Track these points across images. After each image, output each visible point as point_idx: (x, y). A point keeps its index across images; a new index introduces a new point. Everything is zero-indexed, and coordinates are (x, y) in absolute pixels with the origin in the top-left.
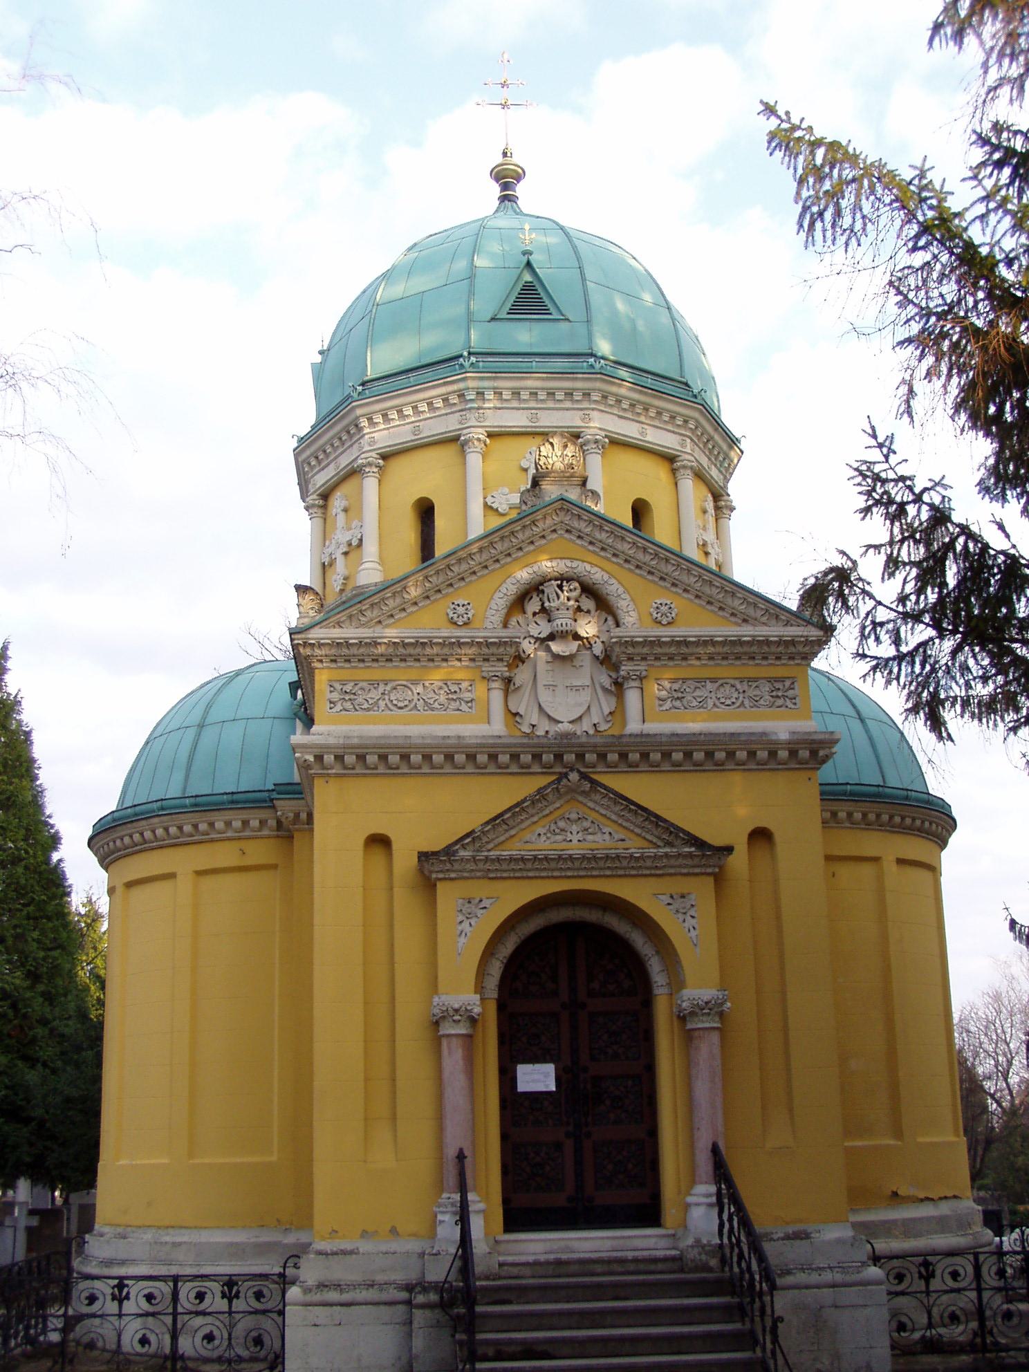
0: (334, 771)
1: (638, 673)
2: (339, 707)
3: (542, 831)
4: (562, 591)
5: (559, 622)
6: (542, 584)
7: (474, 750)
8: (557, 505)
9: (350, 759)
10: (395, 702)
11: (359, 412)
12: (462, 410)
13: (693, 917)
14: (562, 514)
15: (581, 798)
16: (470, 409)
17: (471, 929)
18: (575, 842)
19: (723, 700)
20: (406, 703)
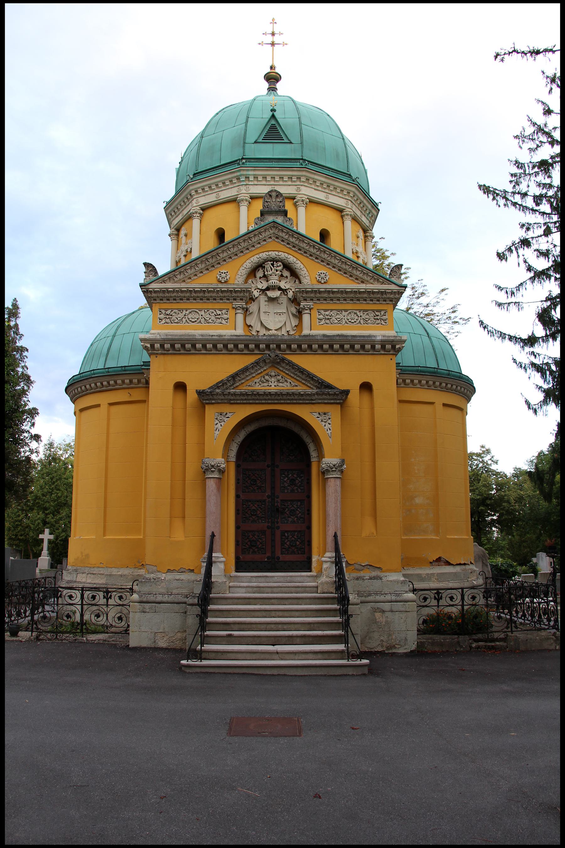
0: (160, 352)
1: (309, 306)
2: (164, 321)
3: (257, 381)
4: (274, 267)
5: (271, 281)
6: (264, 263)
7: (227, 342)
8: (272, 225)
9: (167, 346)
10: (190, 319)
11: (191, 188)
12: (239, 186)
13: (329, 424)
14: (274, 229)
15: (276, 366)
16: (242, 185)
17: (221, 427)
18: (273, 386)
19: (350, 320)
20: (196, 319)
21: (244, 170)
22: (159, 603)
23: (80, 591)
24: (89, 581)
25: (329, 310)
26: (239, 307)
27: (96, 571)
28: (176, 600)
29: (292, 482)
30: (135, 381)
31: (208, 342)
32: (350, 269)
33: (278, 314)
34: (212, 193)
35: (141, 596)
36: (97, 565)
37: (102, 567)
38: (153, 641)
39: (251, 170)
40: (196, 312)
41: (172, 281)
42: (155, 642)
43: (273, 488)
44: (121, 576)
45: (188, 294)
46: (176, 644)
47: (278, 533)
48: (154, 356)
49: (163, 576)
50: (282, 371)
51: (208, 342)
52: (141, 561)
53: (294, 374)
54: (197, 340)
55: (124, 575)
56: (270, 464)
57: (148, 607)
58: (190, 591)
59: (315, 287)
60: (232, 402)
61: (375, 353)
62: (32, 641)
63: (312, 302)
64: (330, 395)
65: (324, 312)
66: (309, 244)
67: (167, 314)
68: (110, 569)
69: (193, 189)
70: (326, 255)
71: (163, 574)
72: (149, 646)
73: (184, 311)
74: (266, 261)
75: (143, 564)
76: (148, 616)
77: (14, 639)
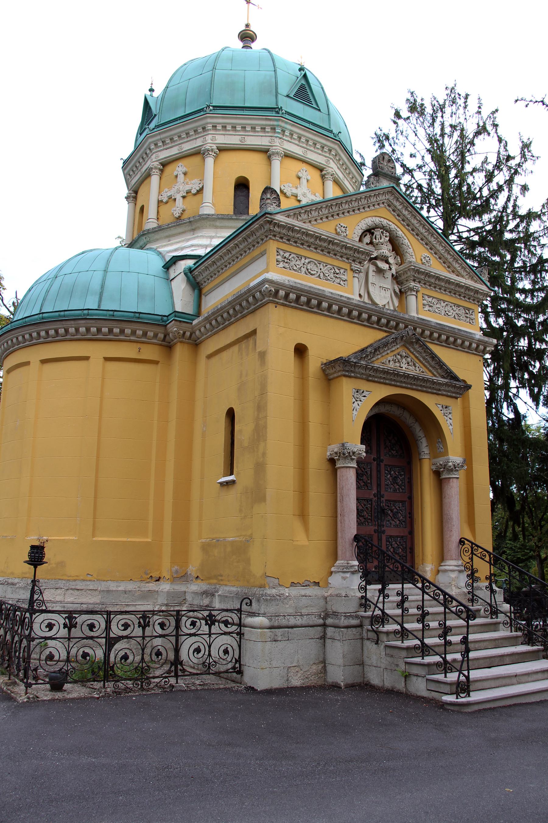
0: (281, 301)
1: (417, 288)
2: (281, 265)
3: (391, 359)
4: (383, 235)
5: (382, 251)
6: (374, 229)
7: (353, 307)
8: (390, 189)
9: (292, 296)
10: (310, 270)
11: (209, 120)
12: (272, 137)
13: (450, 419)
14: (390, 195)
15: (408, 346)
16: (276, 137)
17: (358, 407)
18: (404, 369)
19: (447, 312)
20: (315, 272)
21: (283, 121)
22: (292, 627)
23: (175, 617)
24: (69, 600)
25: (431, 297)
26: (357, 270)
27: (80, 585)
28: (311, 623)
29: (395, 479)
30: (150, 334)
31: (336, 302)
32: (451, 260)
33: (384, 289)
34: (235, 135)
35: (270, 620)
36: (82, 578)
37: (90, 580)
38: (285, 679)
39: (290, 124)
40: (315, 264)
41: (296, 218)
42: (288, 680)
43: (379, 485)
44: (125, 592)
45: (312, 240)
46: (311, 680)
47: (384, 538)
48: (274, 305)
49: (286, 592)
50: (412, 353)
51: (336, 302)
52: (149, 572)
53: (424, 358)
54: (325, 297)
55: (130, 591)
56: (376, 457)
57: (280, 634)
58: (321, 610)
59: (428, 269)
60: (370, 378)
61: (469, 351)
62: (110, 695)
63: (418, 284)
64: (455, 387)
65: (428, 299)
66: (420, 221)
67: (285, 257)
68: (103, 584)
69: (210, 123)
70: (432, 238)
71: (286, 589)
72: (282, 686)
73: (303, 259)
74: (376, 227)
75: (151, 576)
76: (280, 645)
77: (58, 695)
